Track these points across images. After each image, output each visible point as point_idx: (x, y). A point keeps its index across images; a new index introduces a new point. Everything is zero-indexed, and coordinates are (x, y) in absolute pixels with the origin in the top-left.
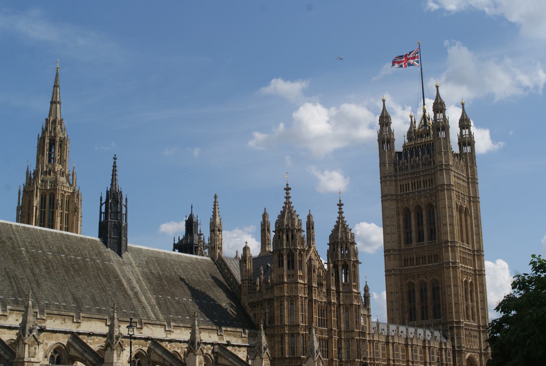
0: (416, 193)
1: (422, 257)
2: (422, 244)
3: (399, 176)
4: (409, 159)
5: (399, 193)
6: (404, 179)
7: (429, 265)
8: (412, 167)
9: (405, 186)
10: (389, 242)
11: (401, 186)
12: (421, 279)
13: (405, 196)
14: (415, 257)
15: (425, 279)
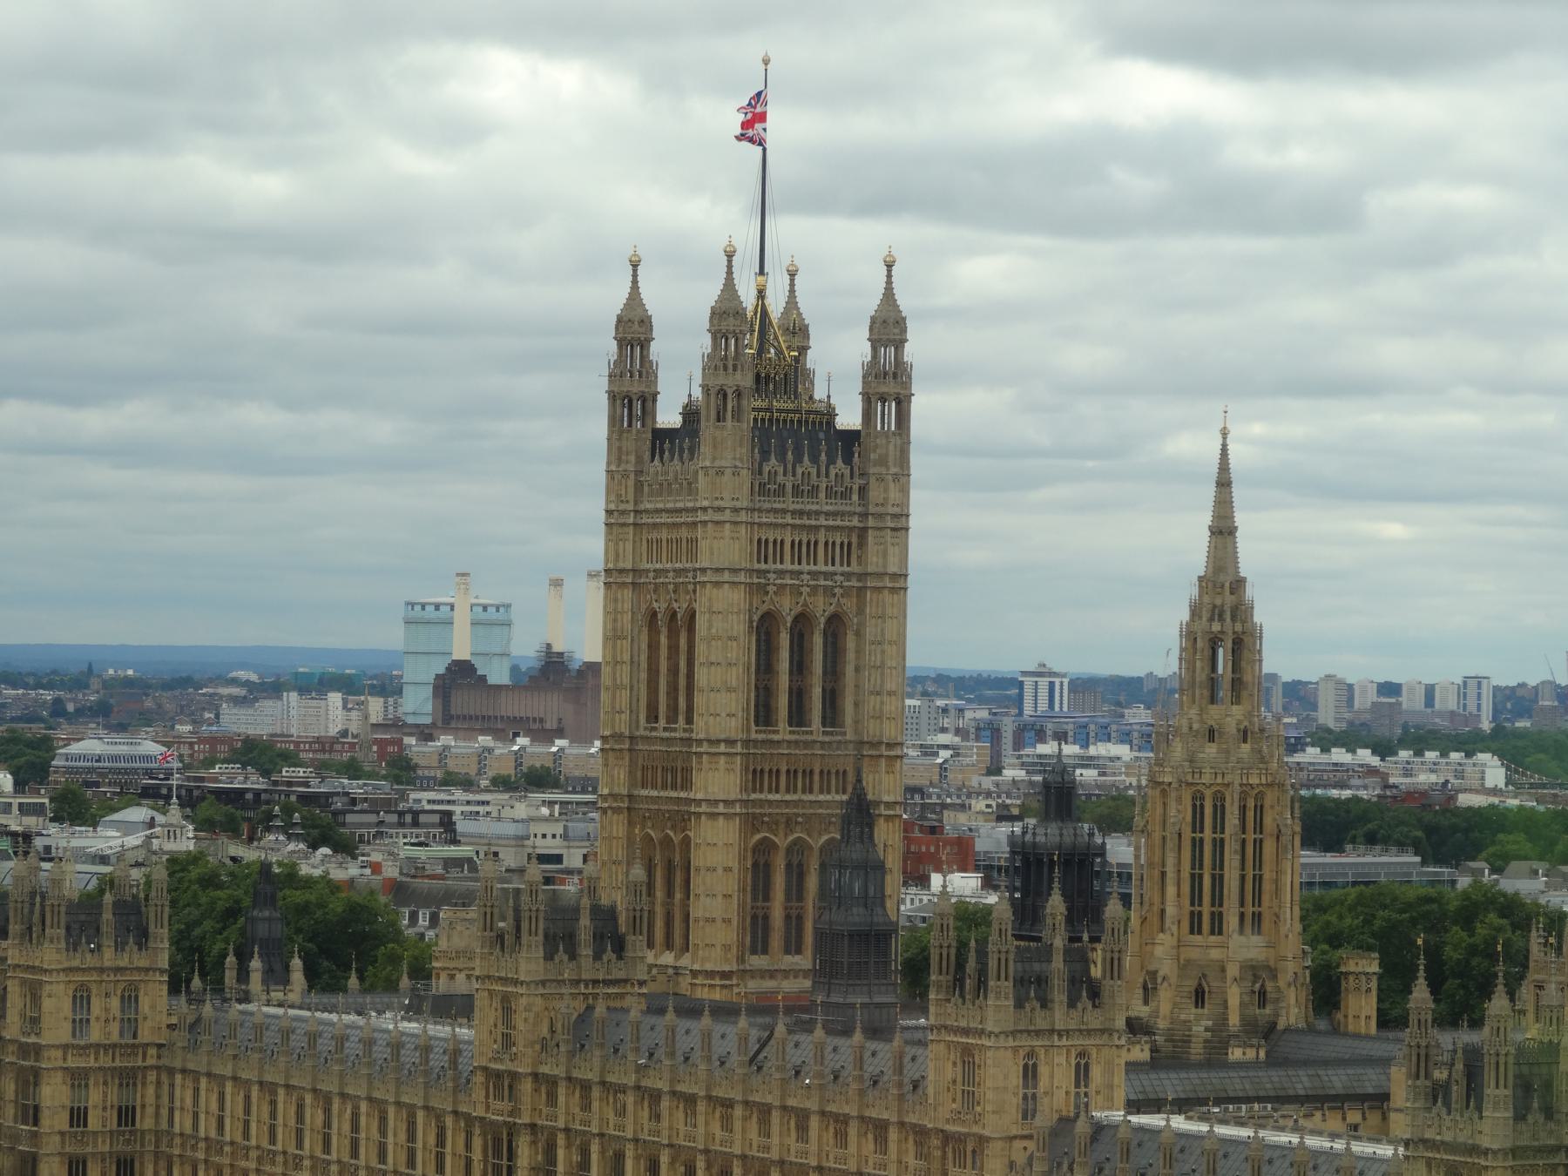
0: (806, 577)
1: (804, 771)
2: (807, 733)
3: (760, 510)
4: (790, 467)
5: (757, 566)
6: (776, 525)
7: (821, 797)
8: (797, 491)
9: (771, 545)
10: (734, 715)
11: (759, 541)
12: (796, 835)
13: (772, 576)
14: (784, 769)
15: (806, 837)
